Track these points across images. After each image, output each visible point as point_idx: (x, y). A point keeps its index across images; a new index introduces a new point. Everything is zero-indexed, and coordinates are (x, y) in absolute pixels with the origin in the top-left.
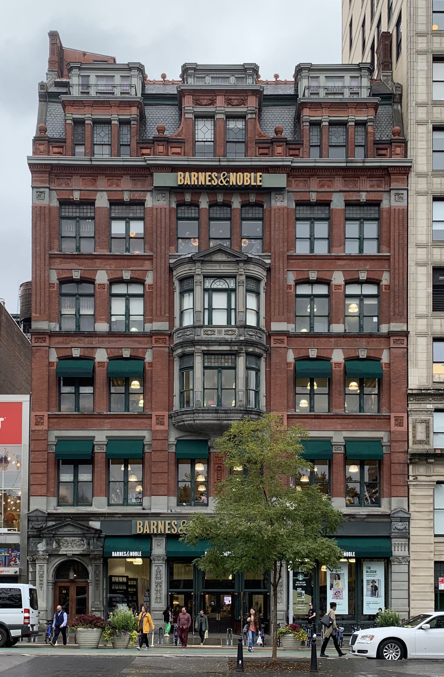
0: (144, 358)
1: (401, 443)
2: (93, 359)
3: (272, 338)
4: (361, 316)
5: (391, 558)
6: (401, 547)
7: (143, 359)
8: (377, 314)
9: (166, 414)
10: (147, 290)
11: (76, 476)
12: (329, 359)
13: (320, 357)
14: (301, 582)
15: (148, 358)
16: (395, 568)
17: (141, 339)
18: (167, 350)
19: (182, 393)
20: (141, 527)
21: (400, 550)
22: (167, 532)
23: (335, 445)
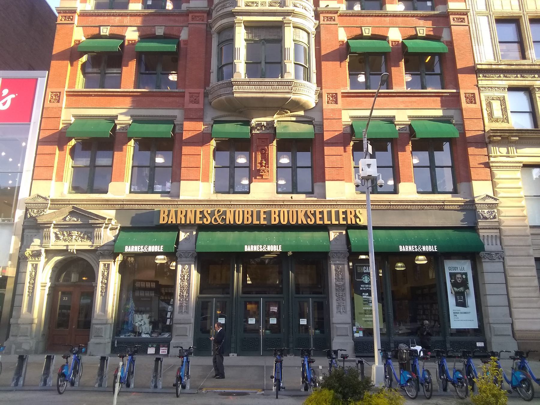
0: (179, 37)
1: (475, 121)
2: (122, 37)
3: (321, 17)
5: (482, 254)
7: (179, 37)
9: (202, 91)
12: (384, 38)
13: (375, 35)
14: (366, 286)
15: (184, 35)
16: (487, 266)
17: (177, 18)
18: (204, 27)
19: (220, 69)
20: (165, 216)
21: (490, 243)
22: (198, 222)
23: (399, 125)
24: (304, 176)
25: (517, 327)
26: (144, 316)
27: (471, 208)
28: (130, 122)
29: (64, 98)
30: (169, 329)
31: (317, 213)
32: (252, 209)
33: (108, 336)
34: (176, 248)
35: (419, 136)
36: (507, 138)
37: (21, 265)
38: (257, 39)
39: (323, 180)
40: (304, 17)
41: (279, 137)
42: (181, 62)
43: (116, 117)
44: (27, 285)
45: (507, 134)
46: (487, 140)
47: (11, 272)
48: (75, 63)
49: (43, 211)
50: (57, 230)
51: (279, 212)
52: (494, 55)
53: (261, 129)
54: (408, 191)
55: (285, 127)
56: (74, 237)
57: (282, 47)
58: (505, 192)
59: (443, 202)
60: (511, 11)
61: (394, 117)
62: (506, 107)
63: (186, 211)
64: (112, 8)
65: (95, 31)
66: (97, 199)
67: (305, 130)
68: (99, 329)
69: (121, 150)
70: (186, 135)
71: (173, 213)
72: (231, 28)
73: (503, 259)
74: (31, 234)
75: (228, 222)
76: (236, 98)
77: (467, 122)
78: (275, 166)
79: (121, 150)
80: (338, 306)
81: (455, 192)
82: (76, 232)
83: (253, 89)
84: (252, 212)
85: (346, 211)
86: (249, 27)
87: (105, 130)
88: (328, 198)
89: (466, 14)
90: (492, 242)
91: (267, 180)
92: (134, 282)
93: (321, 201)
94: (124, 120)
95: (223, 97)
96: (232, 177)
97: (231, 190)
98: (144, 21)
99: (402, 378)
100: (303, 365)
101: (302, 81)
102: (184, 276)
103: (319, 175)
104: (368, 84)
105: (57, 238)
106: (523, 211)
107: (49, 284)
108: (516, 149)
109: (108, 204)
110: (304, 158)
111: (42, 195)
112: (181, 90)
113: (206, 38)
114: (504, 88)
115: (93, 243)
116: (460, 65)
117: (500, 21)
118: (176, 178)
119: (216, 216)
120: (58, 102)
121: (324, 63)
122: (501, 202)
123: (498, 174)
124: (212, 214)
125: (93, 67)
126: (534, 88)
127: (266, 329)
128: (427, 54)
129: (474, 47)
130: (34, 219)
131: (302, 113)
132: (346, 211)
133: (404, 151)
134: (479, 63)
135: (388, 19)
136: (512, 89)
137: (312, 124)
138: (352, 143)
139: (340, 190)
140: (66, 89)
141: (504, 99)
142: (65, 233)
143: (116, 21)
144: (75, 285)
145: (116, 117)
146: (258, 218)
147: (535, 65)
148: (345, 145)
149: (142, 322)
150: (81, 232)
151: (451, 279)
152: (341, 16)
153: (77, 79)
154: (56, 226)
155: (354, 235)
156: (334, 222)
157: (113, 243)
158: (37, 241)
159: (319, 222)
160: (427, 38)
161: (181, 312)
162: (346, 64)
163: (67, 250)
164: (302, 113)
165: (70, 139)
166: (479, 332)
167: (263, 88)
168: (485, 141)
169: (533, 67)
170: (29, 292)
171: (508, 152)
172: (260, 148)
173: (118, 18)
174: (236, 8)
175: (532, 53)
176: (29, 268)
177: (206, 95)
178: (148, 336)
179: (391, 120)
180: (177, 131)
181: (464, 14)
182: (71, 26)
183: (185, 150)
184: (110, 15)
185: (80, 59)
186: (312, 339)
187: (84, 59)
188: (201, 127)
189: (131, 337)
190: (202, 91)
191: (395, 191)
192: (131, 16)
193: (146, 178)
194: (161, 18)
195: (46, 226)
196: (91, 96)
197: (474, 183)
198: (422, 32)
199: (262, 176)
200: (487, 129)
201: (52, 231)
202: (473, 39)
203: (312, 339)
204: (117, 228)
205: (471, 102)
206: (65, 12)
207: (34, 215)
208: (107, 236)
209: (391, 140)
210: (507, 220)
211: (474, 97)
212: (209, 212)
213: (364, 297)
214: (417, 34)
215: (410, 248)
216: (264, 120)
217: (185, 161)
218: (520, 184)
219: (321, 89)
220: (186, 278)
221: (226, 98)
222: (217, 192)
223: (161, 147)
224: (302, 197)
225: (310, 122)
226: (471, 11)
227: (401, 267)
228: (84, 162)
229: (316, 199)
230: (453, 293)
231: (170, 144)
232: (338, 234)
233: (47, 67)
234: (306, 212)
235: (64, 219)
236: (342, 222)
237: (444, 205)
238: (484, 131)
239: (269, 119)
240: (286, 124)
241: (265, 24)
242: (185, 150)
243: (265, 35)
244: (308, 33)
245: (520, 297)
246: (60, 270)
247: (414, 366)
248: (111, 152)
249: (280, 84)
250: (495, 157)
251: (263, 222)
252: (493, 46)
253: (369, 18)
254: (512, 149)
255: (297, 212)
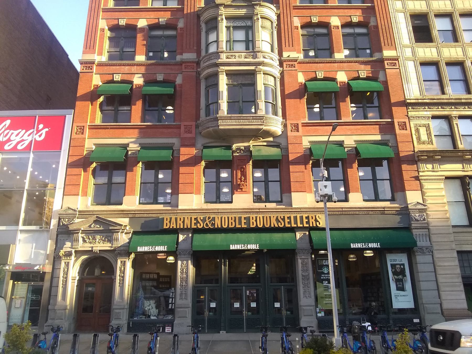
0: (175, 81)
1: (407, 143)
2: (131, 83)
4: (357, 49)
5: (415, 249)
6: (423, 237)
7: (174, 82)
8: (368, 47)
9: (194, 123)
10: (179, 31)
11: (110, 178)
12: (334, 80)
14: (326, 275)
15: (179, 80)
16: (420, 258)
17: (173, 67)
19: (208, 106)
20: (168, 222)
22: (193, 226)
24: (275, 188)
25: (445, 306)
26: (151, 301)
27: (405, 212)
28: (139, 149)
29: (87, 131)
30: (172, 312)
31: (286, 218)
32: (235, 216)
33: (125, 319)
34: (177, 248)
35: (363, 156)
36: (432, 157)
37: (56, 263)
38: (235, 83)
39: (290, 192)
40: (271, 66)
41: (254, 159)
42: (177, 102)
43: (128, 145)
44: (61, 279)
45: (432, 154)
46: (416, 159)
47: (48, 269)
48: (94, 103)
49: (73, 220)
50: (84, 235)
51: (256, 217)
52: (420, 91)
53: (240, 152)
54: (356, 200)
55: (259, 150)
56: (97, 240)
57: (255, 89)
58: (432, 199)
59: (384, 208)
60: (431, 57)
61: (343, 141)
62: (430, 132)
63: (184, 218)
64: (122, 59)
65: (110, 78)
66: (114, 209)
67: (274, 152)
68: (119, 313)
69: (132, 171)
70: (182, 158)
71: (173, 220)
72: (216, 75)
73: (432, 252)
74: (63, 238)
75: (216, 227)
76: (221, 129)
77: (400, 145)
78: (252, 181)
79: (132, 171)
80: (305, 292)
81: (393, 200)
82: (99, 236)
83: (233, 122)
84: (235, 218)
85: (308, 216)
86: (229, 74)
87: (119, 156)
88: (293, 206)
89: (397, 60)
90: (423, 239)
91: (246, 192)
92: (142, 274)
93: (288, 209)
94: (134, 147)
95: (211, 129)
96: (218, 190)
97: (218, 200)
98: (146, 70)
99: (355, 347)
100: (282, 339)
101: (271, 115)
102: (183, 270)
103: (286, 188)
104: (322, 115)
105: (84, 241)
106: (446, 214)
107: (78, 278)
108: (439, 165)
109: (124, 214)
110: (274, 174)
111: (72, 208)
112: (178, 123)
113: (197, 83)
114: (429, 117)
115: (112, 245)
116: (393, 100)
117: (423, 64)
118: (176, 192)
119: (207, 221)
120: (83, 134)
121: (287, 100)
122: (429, 208)
123: (427, 185)
124: (204, 220)
125: (108, 105)
126: (452, 117)
127: (248, 312)
128: (368, 92)
129: (404, 85)
130: (67, 226)
131: (271, 139)
132: (308, 216)
133: (352, 167)
134: (409, 98)
135: (336, 64)
136: (434, 117)
137: (280, 148)
138: (311, 162)
139: (303, 200)
140: (88, 124)
141: (429, 126)
142: (90, 237)
143: (126, 70)
144: (98, 278)
145: (128, 145)
146: (240, 223)
147: (451, 99)
148: (306, 163)
149: (150, 307)
150: (103, 236)
151: (392, 268)
152: (299, 63)
153: (97, 115)
154: (84, 232)
155: (314, 234)
156: (299, 225)
157: (128, 245)
158: (68, 244)
159: (287, 225)
160: (367, 79)
161: (181, 299)
162: (304, 100)
163: (92, 251)
164: (271, 139)
165: (92, 163)
166: (416, 311)
167: (242, 122)
168: (415, 159)
169: (450, 101)
170: (63, 284)
171: (433, 168)
172: (239, 167)
173: (127, 67)
174: (219, 60)
175: (449, 89)
176: (63, 265)
177: (197, 127)
178: (155, 318)
179: (341, 144)
180: (175, 155)
181: (395, 60)
182: (91, 74)
183: (182, 170)
184: (121, 65)
185: (98, 100)
186: (284, 319)
187: (101, 99)
188: (193, 151)
189: (142, 319)
190: (194, 123)
191: (346, 200)
192: (137, 65)
193: (152, 193)
194: (161, 67)
195: (75, 232)
196: (108, 128)
197: (408, 193)
198: (363, 74)
199: (242, 189)
200: (416, 150)
201: (80, 235)
202: (403, 79)
203: (284, 319)
204: (130, 233)
205: (403, 129)
206: (86, 63)
207: (66, 223)
208: (123, 239)
209: (342, 160)
210: (434, 221)
211: (405, 125)
212: (202, 219)
213: (324, 284)
214: (359, 76)
215: (359, 245)
216: (242, 145)
217: (182, 179)
218: (443, 193)
219: (286, 121)
220: (184, 271)
221: (213, 130)
222: (206, 202)
223: (164, 168)
224: (273, 205)
225: (278, 146)
226: (401, 58)
227: (353, 258)
228: (103, 180)
229: (284, 207)
230: (394, 280)
231: (170, 165)
232: (302, 234)
233: (72, 107)
234: (277, 217)
235: (90, 226)
236: (306, 225)
237: (385, 210)
238: (414, 151)
239: (246, 144)
240: (260, 148)
241: (242, 72)
242: (182, 170)
243: (241, 80)
244: (275, 78)
245: (446, 283)
246: (87, 267)
247: (363, 338)
248: (124, 171)
249: (254, 118)
250: (423, 172)
251: (244, 226)
252: (419, 84)
253: (321, 65)
254: (436, 165)
255: (270, 217)
